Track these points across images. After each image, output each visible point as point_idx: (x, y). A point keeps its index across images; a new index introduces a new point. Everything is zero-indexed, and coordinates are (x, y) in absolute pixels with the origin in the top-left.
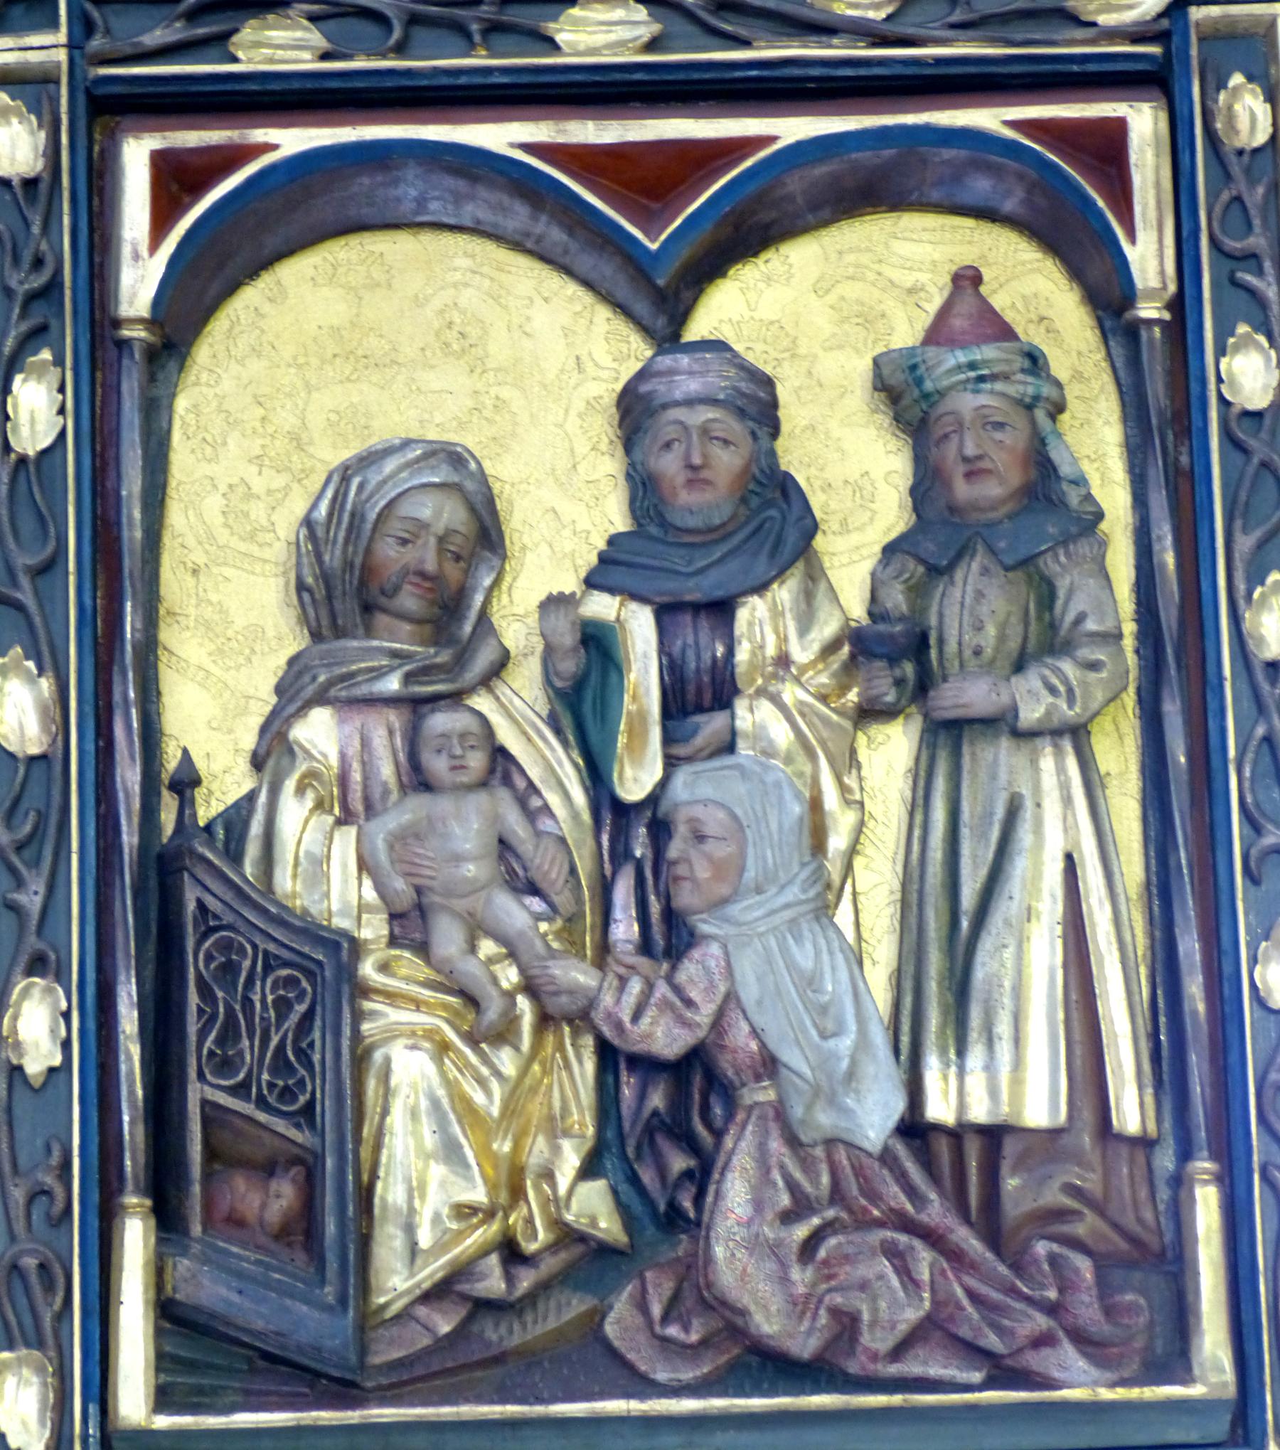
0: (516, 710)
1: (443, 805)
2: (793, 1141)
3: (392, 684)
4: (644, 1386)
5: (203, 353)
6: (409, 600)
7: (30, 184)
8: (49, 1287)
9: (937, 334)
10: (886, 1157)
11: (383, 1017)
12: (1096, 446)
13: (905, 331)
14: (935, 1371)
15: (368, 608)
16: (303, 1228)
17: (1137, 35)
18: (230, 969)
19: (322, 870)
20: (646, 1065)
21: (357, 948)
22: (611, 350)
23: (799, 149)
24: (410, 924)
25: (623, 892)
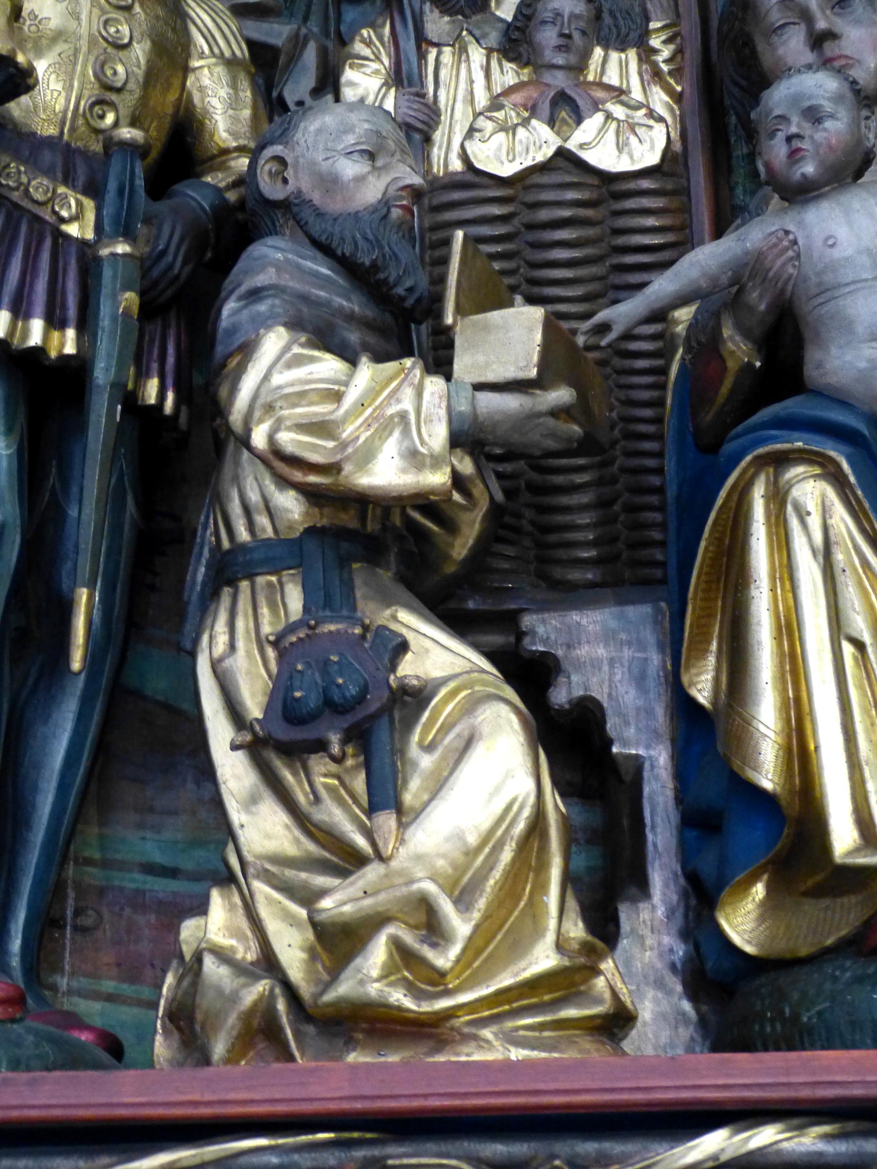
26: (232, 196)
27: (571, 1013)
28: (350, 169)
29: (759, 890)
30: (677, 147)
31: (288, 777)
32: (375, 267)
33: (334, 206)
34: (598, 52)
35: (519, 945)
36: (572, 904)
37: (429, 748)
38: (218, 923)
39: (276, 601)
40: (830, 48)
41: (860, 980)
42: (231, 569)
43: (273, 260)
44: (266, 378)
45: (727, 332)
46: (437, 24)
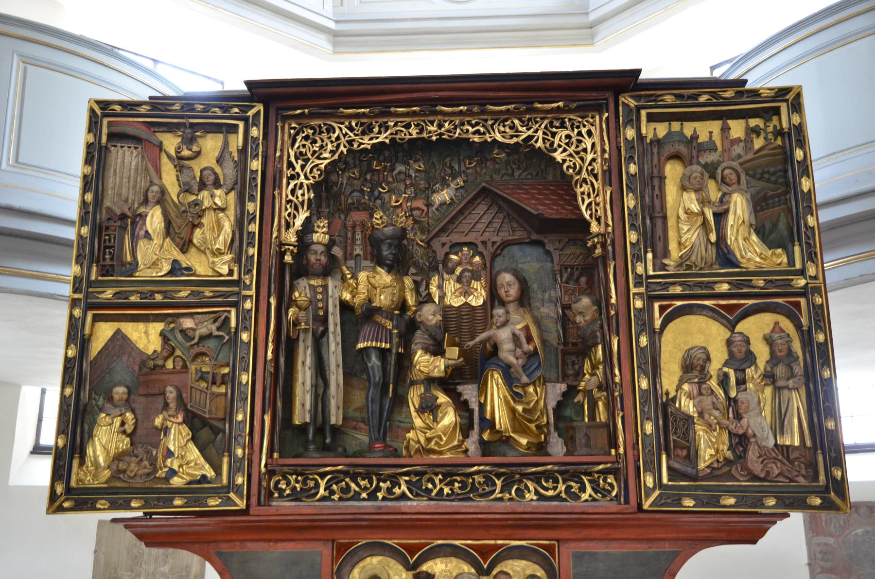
0: (713, 383)
1: (704, 398)
2: (759, 446)
3: (696, 380)
4: (738, 481)
5: (665, 332)
6: (698, 368)
9: (773, 331)
10: (772, 449)
11: (698, 427)
12: (797, 346)
13: (767, 331)
14: (782, 480)
15: (692, 369)
16: (688, 457)
17: (801, 288)
18: (675, 421)
19: (688, 406)
20: (736, 435)
21: (694, 417)
22: (725, 334)
23: (753, 305)
24: (701, 414)
25: (731, 410)
28: (431, 317)
33: (429, 324)
35: (453, 441)
38: (411, 435)
42: (413, 383)
43: (419, 337)
46: (446, 276)
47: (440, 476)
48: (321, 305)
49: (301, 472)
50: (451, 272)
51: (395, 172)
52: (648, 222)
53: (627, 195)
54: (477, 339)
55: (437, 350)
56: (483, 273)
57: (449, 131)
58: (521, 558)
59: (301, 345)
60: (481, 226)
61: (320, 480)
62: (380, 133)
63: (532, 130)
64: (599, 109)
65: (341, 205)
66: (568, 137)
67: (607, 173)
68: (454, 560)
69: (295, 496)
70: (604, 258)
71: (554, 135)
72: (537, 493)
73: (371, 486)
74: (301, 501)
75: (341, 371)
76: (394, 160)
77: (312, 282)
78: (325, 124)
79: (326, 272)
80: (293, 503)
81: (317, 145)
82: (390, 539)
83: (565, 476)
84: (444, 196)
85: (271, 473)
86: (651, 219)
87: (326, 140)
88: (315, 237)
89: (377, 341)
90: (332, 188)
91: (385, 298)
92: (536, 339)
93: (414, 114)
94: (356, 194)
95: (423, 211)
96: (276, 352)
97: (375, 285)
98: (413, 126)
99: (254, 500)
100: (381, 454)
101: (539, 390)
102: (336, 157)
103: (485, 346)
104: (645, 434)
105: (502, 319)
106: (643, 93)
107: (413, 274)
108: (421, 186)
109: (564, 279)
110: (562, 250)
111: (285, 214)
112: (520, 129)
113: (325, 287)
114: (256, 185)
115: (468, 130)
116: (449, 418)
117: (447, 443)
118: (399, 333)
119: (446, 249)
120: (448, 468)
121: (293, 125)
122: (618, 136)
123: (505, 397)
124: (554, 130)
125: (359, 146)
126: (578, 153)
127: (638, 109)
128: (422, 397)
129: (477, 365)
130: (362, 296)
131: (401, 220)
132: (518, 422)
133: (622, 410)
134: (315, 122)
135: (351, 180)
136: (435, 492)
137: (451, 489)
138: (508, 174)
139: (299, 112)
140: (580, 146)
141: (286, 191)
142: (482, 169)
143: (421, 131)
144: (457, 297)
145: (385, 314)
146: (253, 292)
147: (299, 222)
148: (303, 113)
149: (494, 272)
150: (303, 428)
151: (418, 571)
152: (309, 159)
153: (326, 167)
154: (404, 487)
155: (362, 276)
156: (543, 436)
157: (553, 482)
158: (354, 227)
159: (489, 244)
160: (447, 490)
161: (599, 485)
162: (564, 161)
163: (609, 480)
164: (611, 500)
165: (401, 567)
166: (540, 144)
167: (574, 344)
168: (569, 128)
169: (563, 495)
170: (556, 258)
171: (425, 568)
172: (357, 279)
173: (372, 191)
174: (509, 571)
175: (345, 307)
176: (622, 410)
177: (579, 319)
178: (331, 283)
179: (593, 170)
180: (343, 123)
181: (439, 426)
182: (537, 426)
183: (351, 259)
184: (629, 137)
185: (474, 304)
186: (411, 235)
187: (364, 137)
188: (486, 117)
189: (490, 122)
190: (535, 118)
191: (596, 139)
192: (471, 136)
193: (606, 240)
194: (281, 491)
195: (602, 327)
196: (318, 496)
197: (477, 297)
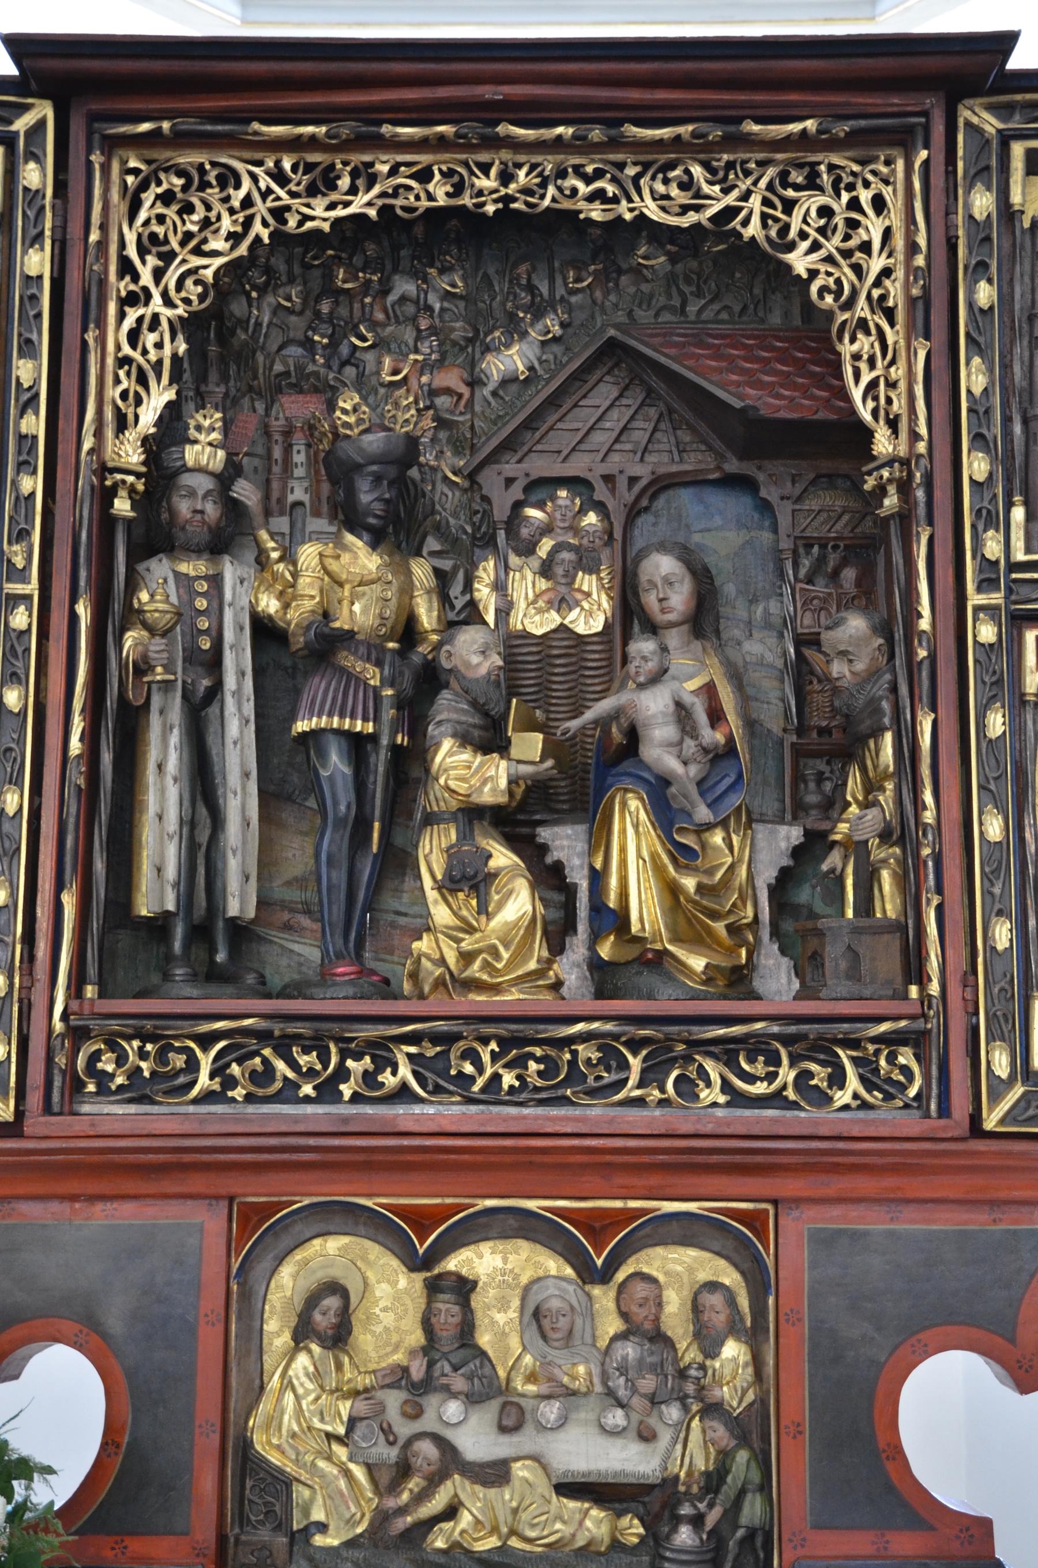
7: (991, 645)
8: (1007, 1021)
26: (430, 657)
27: (541, 983)
28: (475, 659)
29: (612, 938)
30: (610, 620)
31: (450, 899)
32: (484, 704)
33: (471, 674)
34: (580, 573)
35: (525, 961)
36: (544, 944)
37: (498, 893)
38: (424, 945)
39: (448, 835)
40: (665, 604)
41: (637, 973)
42: (430, 819)
43: (448, 708)
44: (444, 759)
45: (614, 730)
46: (514, 560)
47: (493, 1046)
48: (204, 624)
49: (152, 1032)
50: (528, 550)
51: (392, 298)
52: (1018, 429)
53: (968, 363)
54: (589, 715)
55: (491, 739)
56: (605, 555)
57: (527, 191)
58: (686, 1242)
59: (155, 721)
60: (601, 439)
61: (198, 1051)
62: (353, 190)
63: (735, 193)
64: (904, 139)
65: (255, 377)
66: (825, 211)
67: (920, 305)
68: (522, 1243)
69: (138, 1091)
70: (905, 518)
71: (789, 206)
72: (727, 1087)
73: (325, 1067)
74: (153, 1102)
75: (253, 787)
76: (389, 267)
77: (184, 568)
78: (214, 164)
79: (219, 544)
80: (133, 1109)
81: (195, 217)
82: (369, 1196)
83: (798, 1048)
84: (511, 360)
85: (78, 1035)
86: (1025, 422)
87: (218, 207)
88: (191, 454)
89: (342, 716)
90: (233, 333)
91: (365, 611)
92: (732, 717)
93: (442, 143)
94: (295, 351)
95: (460, 396)
96: (92, 738)
97: (340, 578)
98: (437, 176)
99: (34, 1100)
100: (351, 991)
101: (735, 840)
102: (243, 250)
103: (606, 732)
104: (994, 949)
105: (651, 665)
106: (1018, 97)
107: (433, 554)
108: (456, 335)
109: (803, 572)
110: (799, 499)
111: (113, 393)
112: (706, 189)
113: (216, 581)
114: (39, 316)
115: (574, 191)
116: (518, 904)
117: (511, 964)
118: (397, 696)
119: (516, 492)
120: (513, 1027)
121: (132, 164)
122: (950, 211)
123: (654, 856)
124: (790, 193)
125: (301, 224)
126: (847, 254)
127: (1005, 139)
128: (451, 853)
129: (588, 776)
130: (308, 605)
131: (406, 415)
132: (687, 917)
133: (939, 890)
134: (188, 159)
135: (281, 313)
136: (480, 1082)
137: (519, 1077)
138: (671, 309)
139: (145, 127)
140: (854, 236)
141: (117, 335)
142: (607, 293)
143: (458, 189)
144: (540, 611)
145: (362, 650)
146: (32, 588)
147: (148, 415)
148: (157, 133)
149: (632, 553)
150: (159, 927)
151: (436, 1271)
152: (173, 255)
153: (216, 274)
154: (405, 1071)
155: (308, 554)
156: (744, 952)
157: (766, 1063)
158: (288, 433)
159: (622, 483)
160: (509, 1079)
161: (876, 1071)
162: (813, 274)
163: (902, 1060)
164: (907, 1106)
165: (395, 1263)
166: (754, 229)
167: (823, 731)
168: (829, 189)
169: (791, 1094)
170: (784, 521)
171: (453, 1263)
172: (295, 563)
173: (334, 344)
174: (655, 1274)
175: (265, 632)
176: (939, 890)
177: (838, 668)
178: (230, 572)
179: (883, 298)
180: (259, 163)
181: (494, 923)
182: (728, 927)
183: (282, 514)
184: (979, 215)
185: (581, 629)
186: (428, 457)
187: (313, 201)
188: (619, 157)
189: (631, 171)
190: (744, 162)
191: (895, 219)
192: (582, 205)
193: (911, 475)
194: (103, 1079)
195: (894, 689)
196: (195, 1092)
197: (590, 613)
